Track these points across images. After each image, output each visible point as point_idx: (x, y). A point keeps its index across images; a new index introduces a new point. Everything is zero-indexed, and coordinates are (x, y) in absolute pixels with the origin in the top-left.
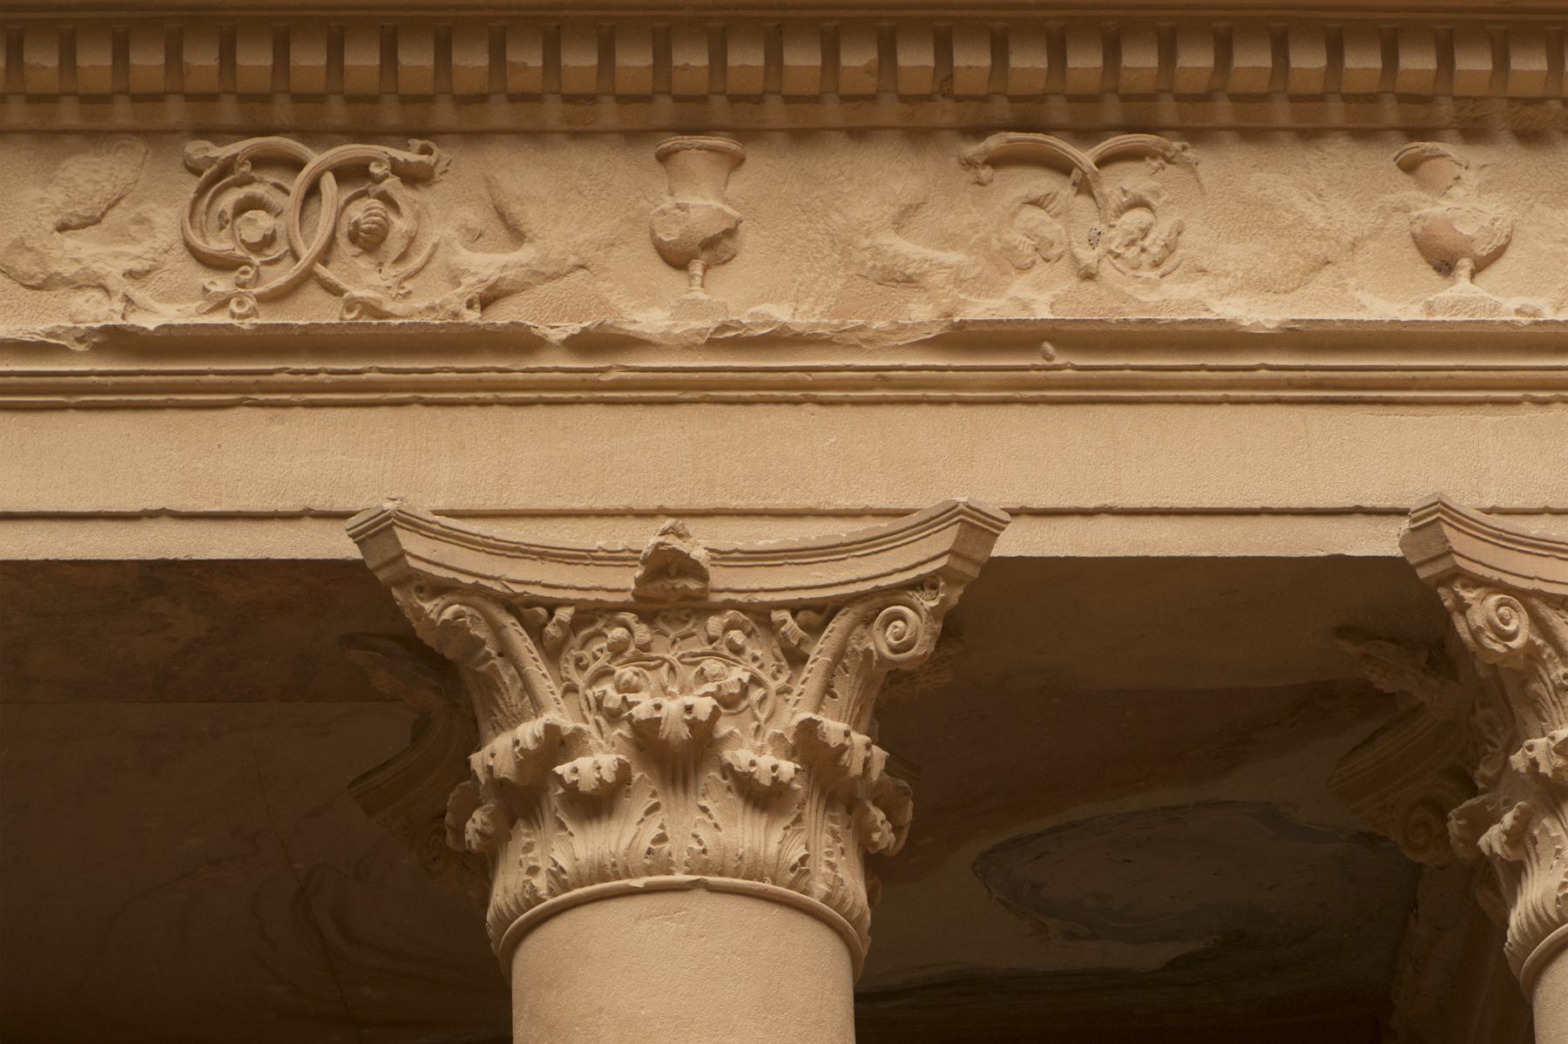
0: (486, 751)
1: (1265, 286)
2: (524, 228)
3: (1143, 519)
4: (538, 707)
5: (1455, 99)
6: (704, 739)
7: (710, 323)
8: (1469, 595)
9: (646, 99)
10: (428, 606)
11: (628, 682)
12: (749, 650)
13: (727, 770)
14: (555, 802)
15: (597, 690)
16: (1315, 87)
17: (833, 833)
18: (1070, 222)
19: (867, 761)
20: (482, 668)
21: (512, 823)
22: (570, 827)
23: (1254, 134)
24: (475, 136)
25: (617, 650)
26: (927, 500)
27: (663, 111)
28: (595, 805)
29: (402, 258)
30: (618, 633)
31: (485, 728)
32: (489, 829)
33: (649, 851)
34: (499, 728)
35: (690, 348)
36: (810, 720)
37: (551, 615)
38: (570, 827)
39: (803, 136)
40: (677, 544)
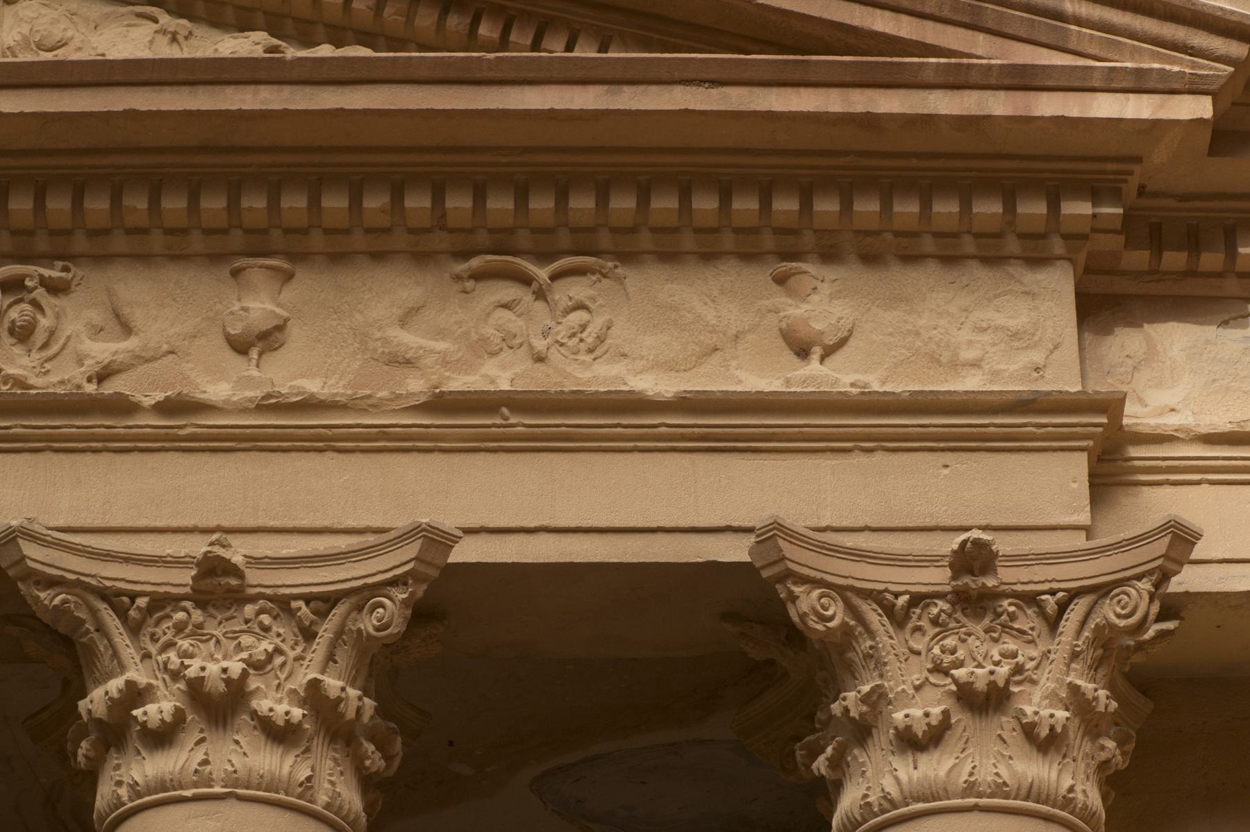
1: (670, 367)
2: (133, 324)
3: (571, 535)
4: (123, 668)
5: (815, 231)
7: (258, 393)
8: (797, 590)
9: (225, 231)
10: (42, 595)
11: (185, 651)
12: (275, 629)
13: (254, 714)
14: (134, 735)
15: (164, 656)
16: (713, 222)
17: (335, 760)
18: (530, 320)
19: (359, 710)
20: (84, 640)
21: (107, 750)
22: (144, 754)
23: (668, 256)
24: (102, 259)
25: (180, 628)
26: (401, 522)
27: (236, 240)
29: (45, 346)
30: (180, 615)
32: (91, 754)
33: (196, 771)
34: (99, 682)
35: (243, 410)
36: (315, 679)
37: (133, 602)
38: (144, 754)
39: (338, 258)
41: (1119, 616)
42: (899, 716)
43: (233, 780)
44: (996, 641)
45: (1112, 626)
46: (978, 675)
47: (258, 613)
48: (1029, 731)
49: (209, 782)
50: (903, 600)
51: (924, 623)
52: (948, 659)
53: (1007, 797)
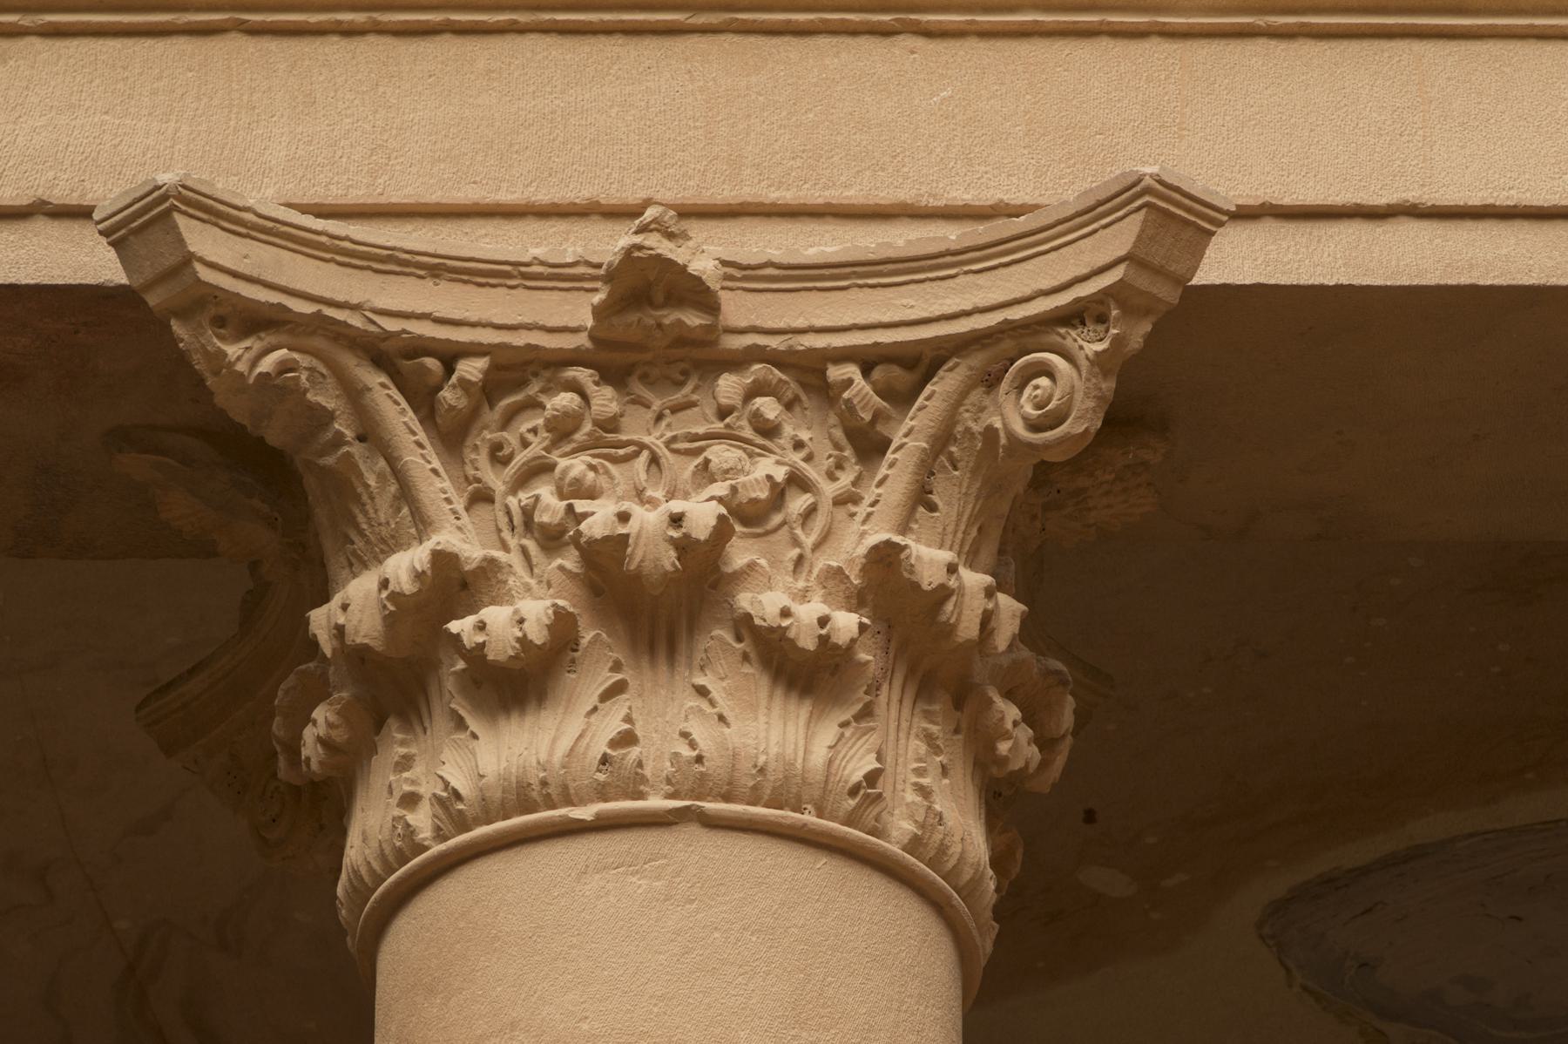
0: (337, 600)
3: (1469, 224)
4: (423, 524)
10: (232, 350)
11: (577, 481)
12: (788, 430)
13: (744, 625)
14: (450, 684)
15: (524, 496)
17: (929, 738)
19: (987, 618)
20: (329, 461)
21: (379, 725)
22: (473, 724)
25: (562, 430)
28: (516, 684)
30: (564, 400)
31: (336, 564)
32: (340, 736)
33: (605, 760)
34: (359, 564)
36: (888, 543)
37: (449, 370)
38: (473, 724)
40: (665, 248)
43: (695, 780)
47: (752, 393)
49: (635, 786)
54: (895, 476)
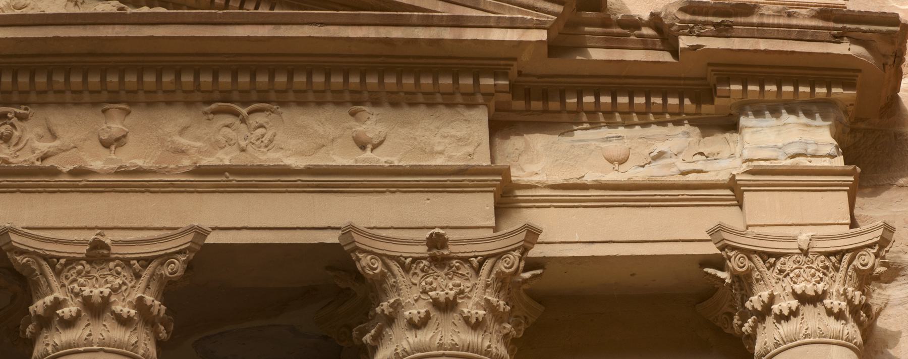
1: (302, 154)
4: (52, 292)
6: (106, 302)
7: (116, 166)
8: (360, 256)
9: (99, 92)
13: (113, 313)
15: (72, 286)
16: (322, 88)
23: (302, 103)
24: (43, 104)
25: (79, 273)
27: (105, 95)
28: (69, 323)
29: (17, 144)
30: (80, 267)
31: (34, 298)
39: (151, 105)
41: (862, 265)
42: (407, 313)
43: (103, 343)
44: (451, 279)
45: (503, 272)
46: (441, 295)
47: (116, 266)
48: (466, 320)
50: (409, 260)
51: (418, 271)
52: (428, 287)
53: (458, 350)
54: (143, 282)
